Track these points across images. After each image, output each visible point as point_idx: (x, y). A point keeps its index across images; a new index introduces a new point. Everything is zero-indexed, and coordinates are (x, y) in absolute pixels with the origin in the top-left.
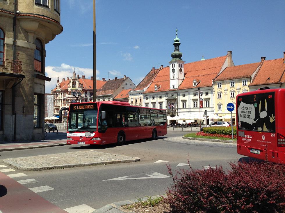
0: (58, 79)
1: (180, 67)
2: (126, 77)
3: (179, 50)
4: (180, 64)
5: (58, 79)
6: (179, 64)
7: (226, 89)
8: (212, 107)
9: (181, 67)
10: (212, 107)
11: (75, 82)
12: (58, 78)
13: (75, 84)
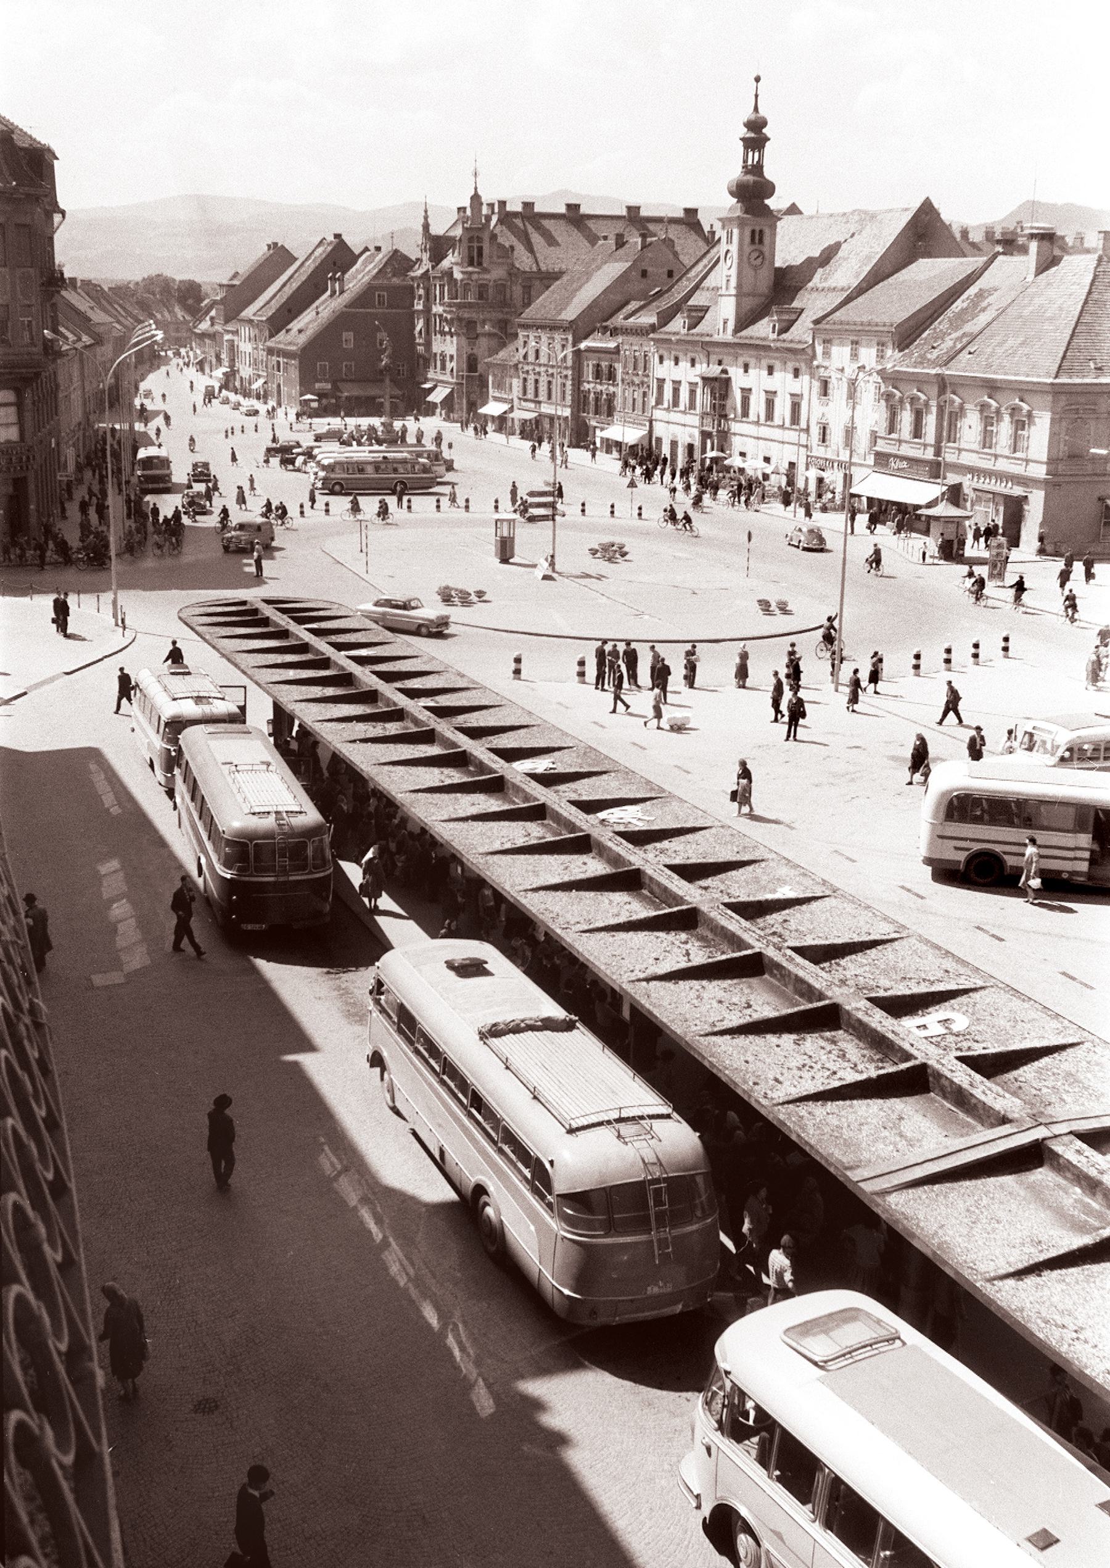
0: (426, 218)
4: (757, 229)
5: (426, 218)
9: (761, 241)
11: (480, 239)
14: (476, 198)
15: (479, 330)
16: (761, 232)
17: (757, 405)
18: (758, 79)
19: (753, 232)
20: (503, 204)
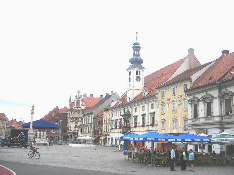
0: (70, 98)
1: (137, 74)
2: (114, 93)
3: (139, 55)
4: (138, 70)
5: (70, 98)
6: (135, 71)
7: (168, 97)
8: (157, 125)
9: (139, 74)
10: (157, 125)
11: (79, 100)
12: (70, 97)
13: (79, 102)
14: (79, 92)
15: (78, 120)
16: (139, 71)
17: (140, 120)
18: (137, 33)
19: (137, 71)
20: (85, 94)
